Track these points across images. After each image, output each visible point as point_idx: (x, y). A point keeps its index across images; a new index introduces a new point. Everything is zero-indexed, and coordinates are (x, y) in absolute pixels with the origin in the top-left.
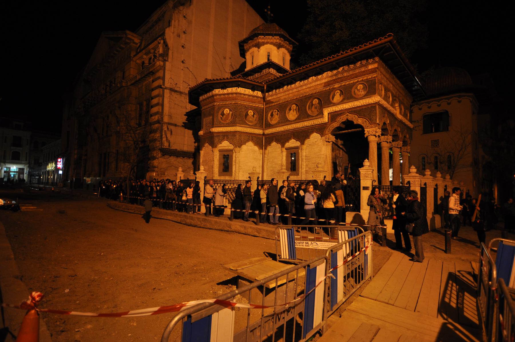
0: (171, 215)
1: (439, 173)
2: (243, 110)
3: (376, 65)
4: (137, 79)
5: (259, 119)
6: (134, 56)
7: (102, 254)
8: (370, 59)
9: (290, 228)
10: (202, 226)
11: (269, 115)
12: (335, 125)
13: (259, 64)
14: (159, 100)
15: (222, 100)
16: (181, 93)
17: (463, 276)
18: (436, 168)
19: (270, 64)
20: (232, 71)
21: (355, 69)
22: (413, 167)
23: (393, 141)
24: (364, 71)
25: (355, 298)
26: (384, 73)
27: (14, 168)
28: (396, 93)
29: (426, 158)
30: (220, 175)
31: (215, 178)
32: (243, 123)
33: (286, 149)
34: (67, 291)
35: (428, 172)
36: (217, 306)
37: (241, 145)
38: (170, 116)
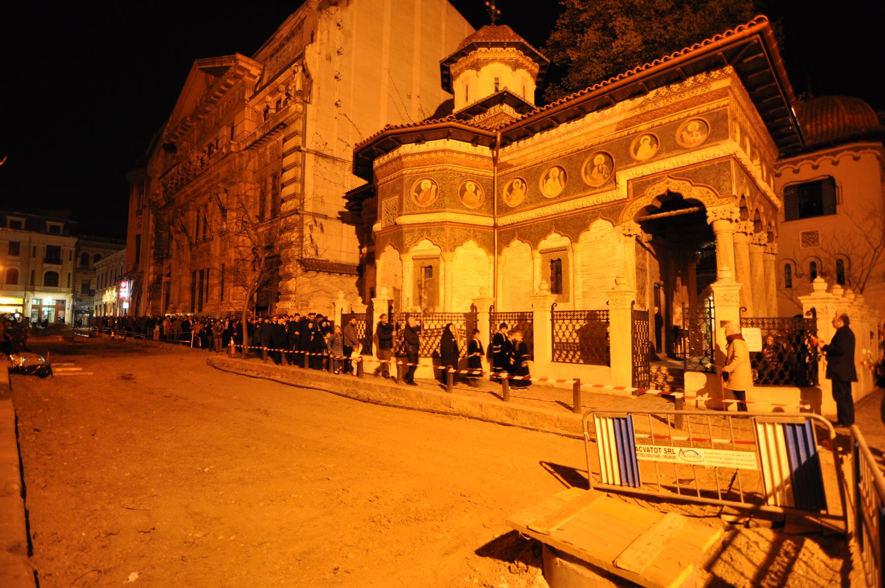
0: (327, 380)
4: (257, 137)
6: (251, 98)
7: (206, 470)
8: (715, 70)
9: (624, 415)
10: (391, 402)
14: (296, 172)
15: (418, 164)
16: (334, 159)
19: (502, 97)
21: (683, 92)
24: (701, 96)
26: (740, 98)
27: (48, 300)
32: (459, 206)
34: (133, 577)
37: (455, 247)
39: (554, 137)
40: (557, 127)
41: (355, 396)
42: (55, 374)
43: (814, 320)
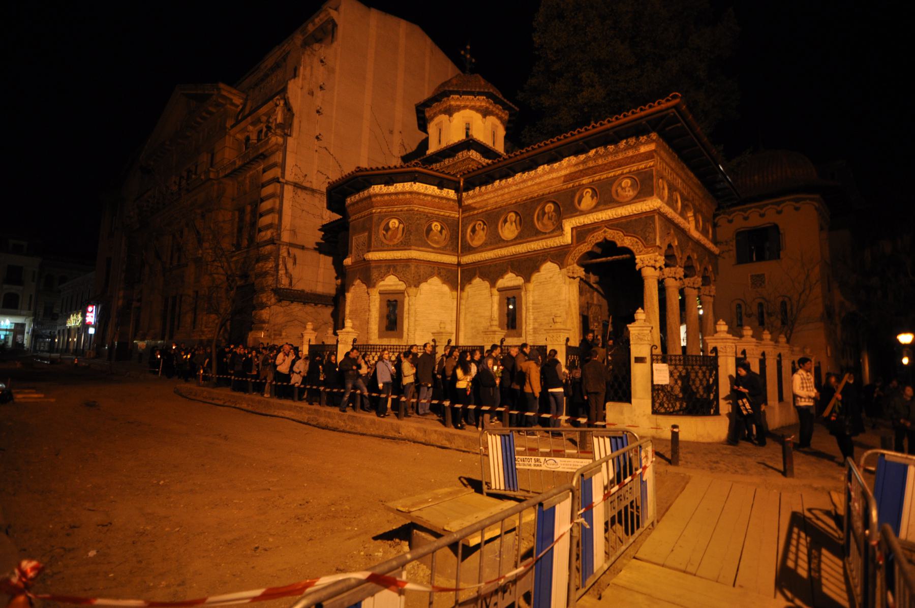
0: (290, 408)
1: (766, 332)
2: (423, 221)
3: (652, 147)
4: (237, 166)
5: (451, 237)
6: (232, 127)
7: (162, 482)
10: (347, 429)
11: (469, 230)
12: (585, 248)
13: (451, 143)
14: (275, 202)
15: (386, 204)
16: (313, 191)
17: (818, 519)
18: (762, 323)
19: (469, 143)
20: (404, 154)
21: (617, 152)
22: (721, 322)
23: (686, 276)
24: (632, 157)
25: (625, 561)
26: (668, 160)
28: (689, 193)
29: (743, 307)
30: (381, 336)
31: (371, 342)
32: (423, 244)
33: (499, 290)
34: (92, 553)
35: (748, 332)
36: (371, 585)
37: (419, 283)
38: (294, 232)
39: (509, 186)
40: (513, 176)
41: (315, 423)
42: (16, 400)
43: (716, 358)
